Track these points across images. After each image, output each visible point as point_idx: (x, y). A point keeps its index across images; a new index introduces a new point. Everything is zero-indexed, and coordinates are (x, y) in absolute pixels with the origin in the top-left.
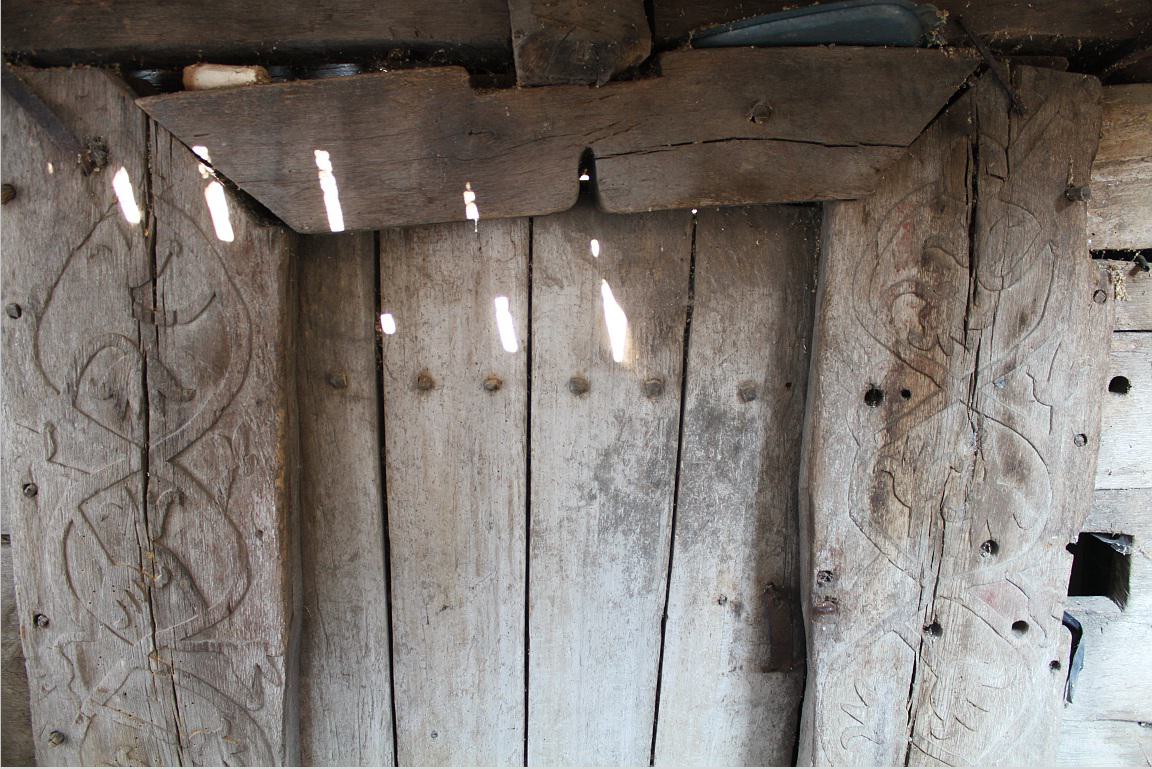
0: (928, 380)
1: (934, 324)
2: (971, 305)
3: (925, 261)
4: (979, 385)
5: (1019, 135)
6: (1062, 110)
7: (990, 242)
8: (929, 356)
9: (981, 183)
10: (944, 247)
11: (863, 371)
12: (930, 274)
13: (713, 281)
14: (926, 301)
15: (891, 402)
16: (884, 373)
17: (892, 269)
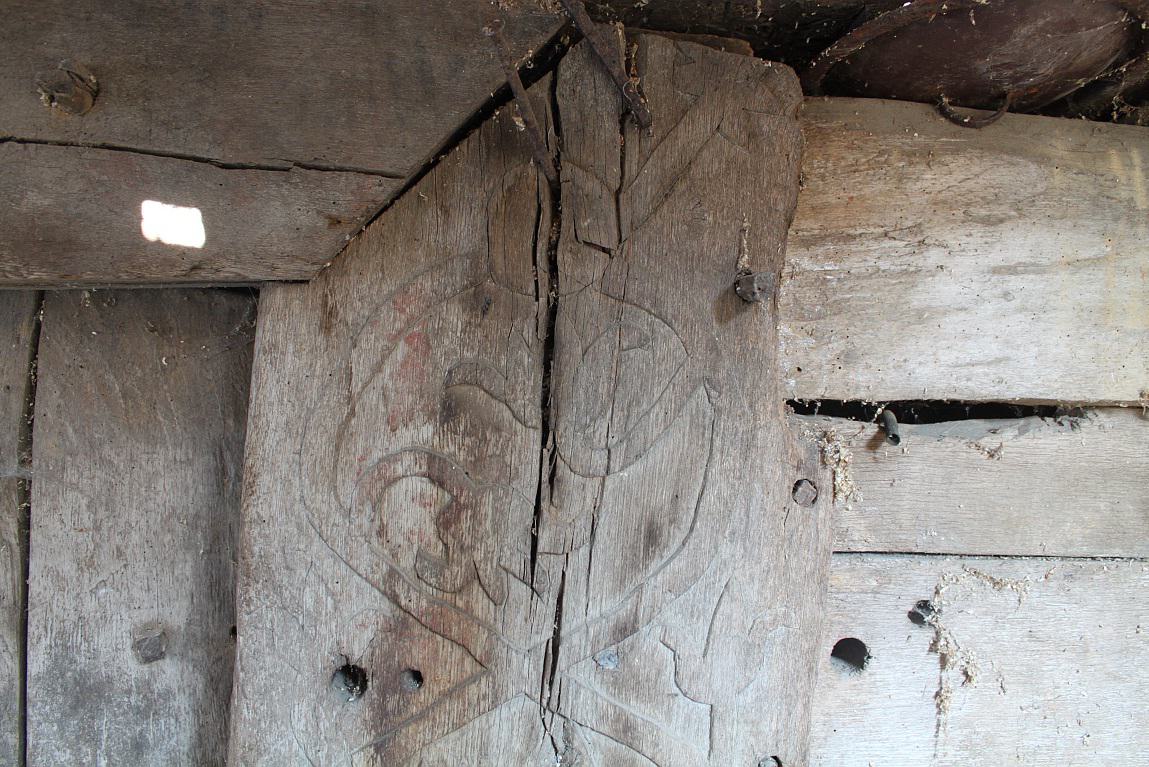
0: (458, 652)
1: (468, 541)
2: (544, 505)
3: (449, 411)
4: (562, 663)
5: (641, 167)
6: (725, 125)
7: (582, 379)
8: (460, 604)
9: (564, 258)
10: (485, 384)
11: (323, 630)
12: (459, 438)
13: (70, 430)
14: (450, 492)
15: (383, 692)
16: (368, 634)
17: (382, 426)
